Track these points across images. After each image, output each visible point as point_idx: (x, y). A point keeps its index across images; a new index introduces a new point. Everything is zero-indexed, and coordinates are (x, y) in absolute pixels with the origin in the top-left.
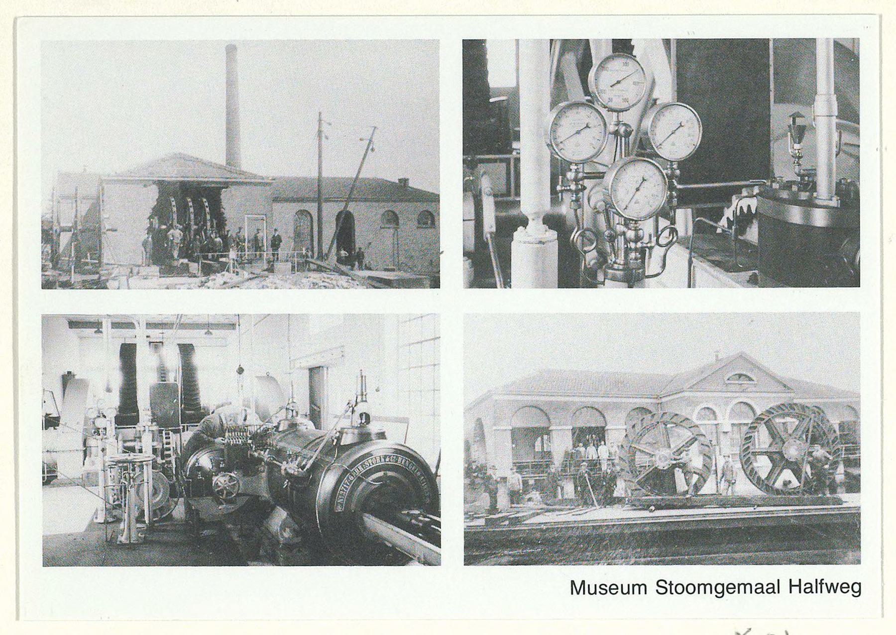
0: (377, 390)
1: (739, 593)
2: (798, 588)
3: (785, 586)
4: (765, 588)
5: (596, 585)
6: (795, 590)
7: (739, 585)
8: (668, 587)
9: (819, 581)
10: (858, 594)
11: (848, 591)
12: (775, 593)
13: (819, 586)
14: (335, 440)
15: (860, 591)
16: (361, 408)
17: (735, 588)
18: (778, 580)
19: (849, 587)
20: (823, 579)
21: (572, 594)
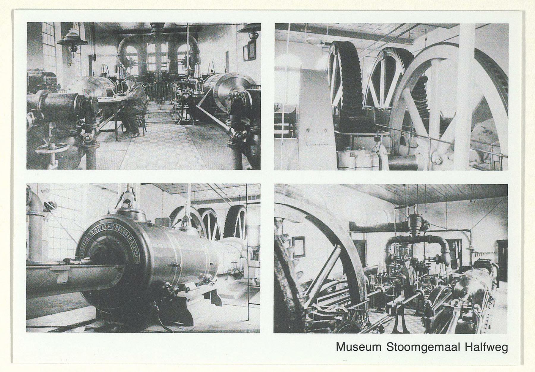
1: (436, 350)
3: (463, 347)
4: (451, 348)
5: (351, 345)
6: (469, 349)
7: (436, 346)
8: (394, 347)
9: (483, 344)
10: (506, 351)
11: (500, 350)
13: (483, 347)
15: (507, 350)
17: (433, 347)
18: (459, 343)
19: (500, 348)
21: (337, 350)
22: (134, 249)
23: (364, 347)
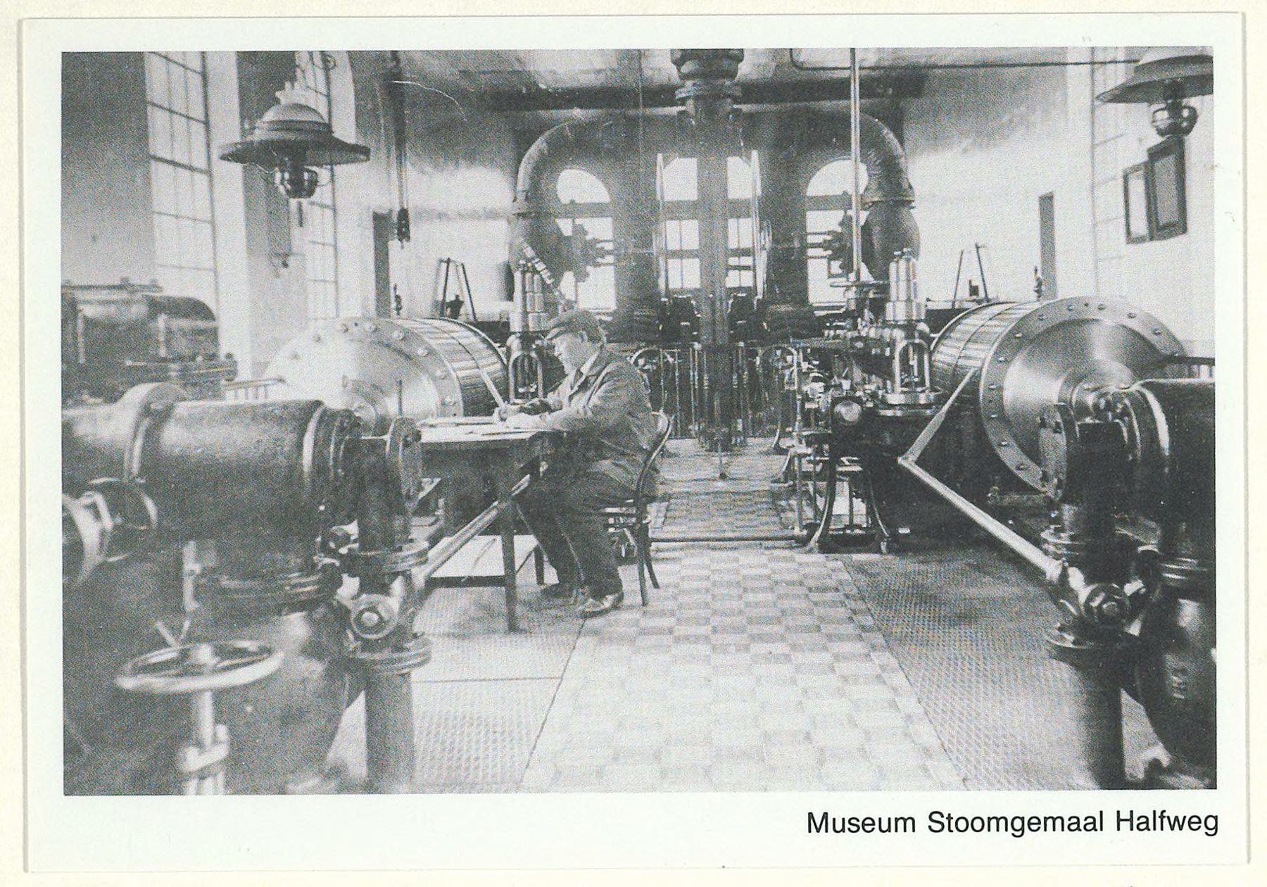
1: (1045, 830)
2: (1129, 823)
3: (1110, 821)
4: (1082, 823)
5: (843, 819)
6: (1125, 826)
7: (1046, 819)
8: (946, 822)
9: (1158, 814)
11: (1199, 827)
12: (1096, 830)
13: (1158, 821)
15: (1216, 828)
17: (1039, 823)
18: (1101, 812)
19: (1200, 822)
20: (1164, 811)
21: (810, 831)
23: (874, 824)
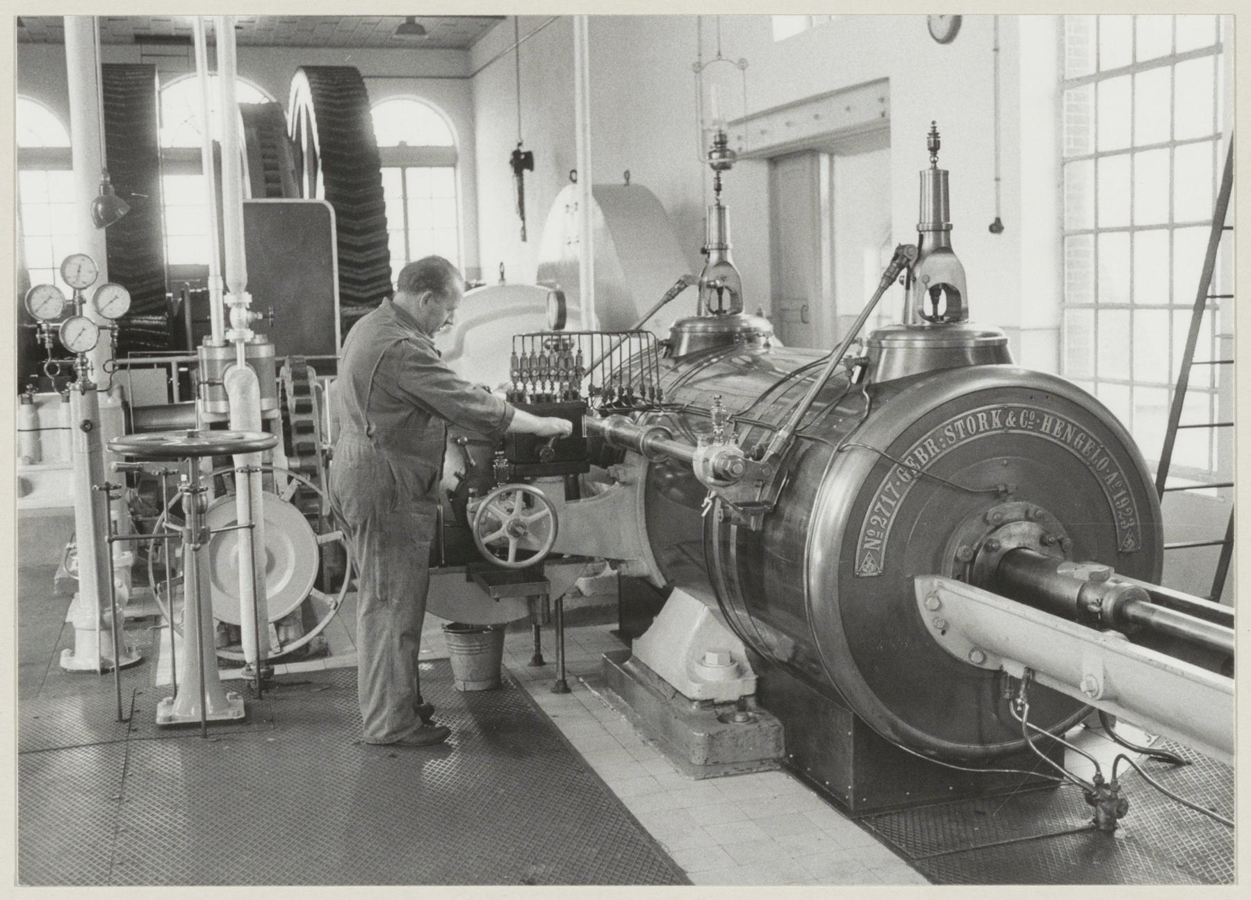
0: (996, 227)
14: (857, 370)
16: (936, 269)
22: (1119, 499)
